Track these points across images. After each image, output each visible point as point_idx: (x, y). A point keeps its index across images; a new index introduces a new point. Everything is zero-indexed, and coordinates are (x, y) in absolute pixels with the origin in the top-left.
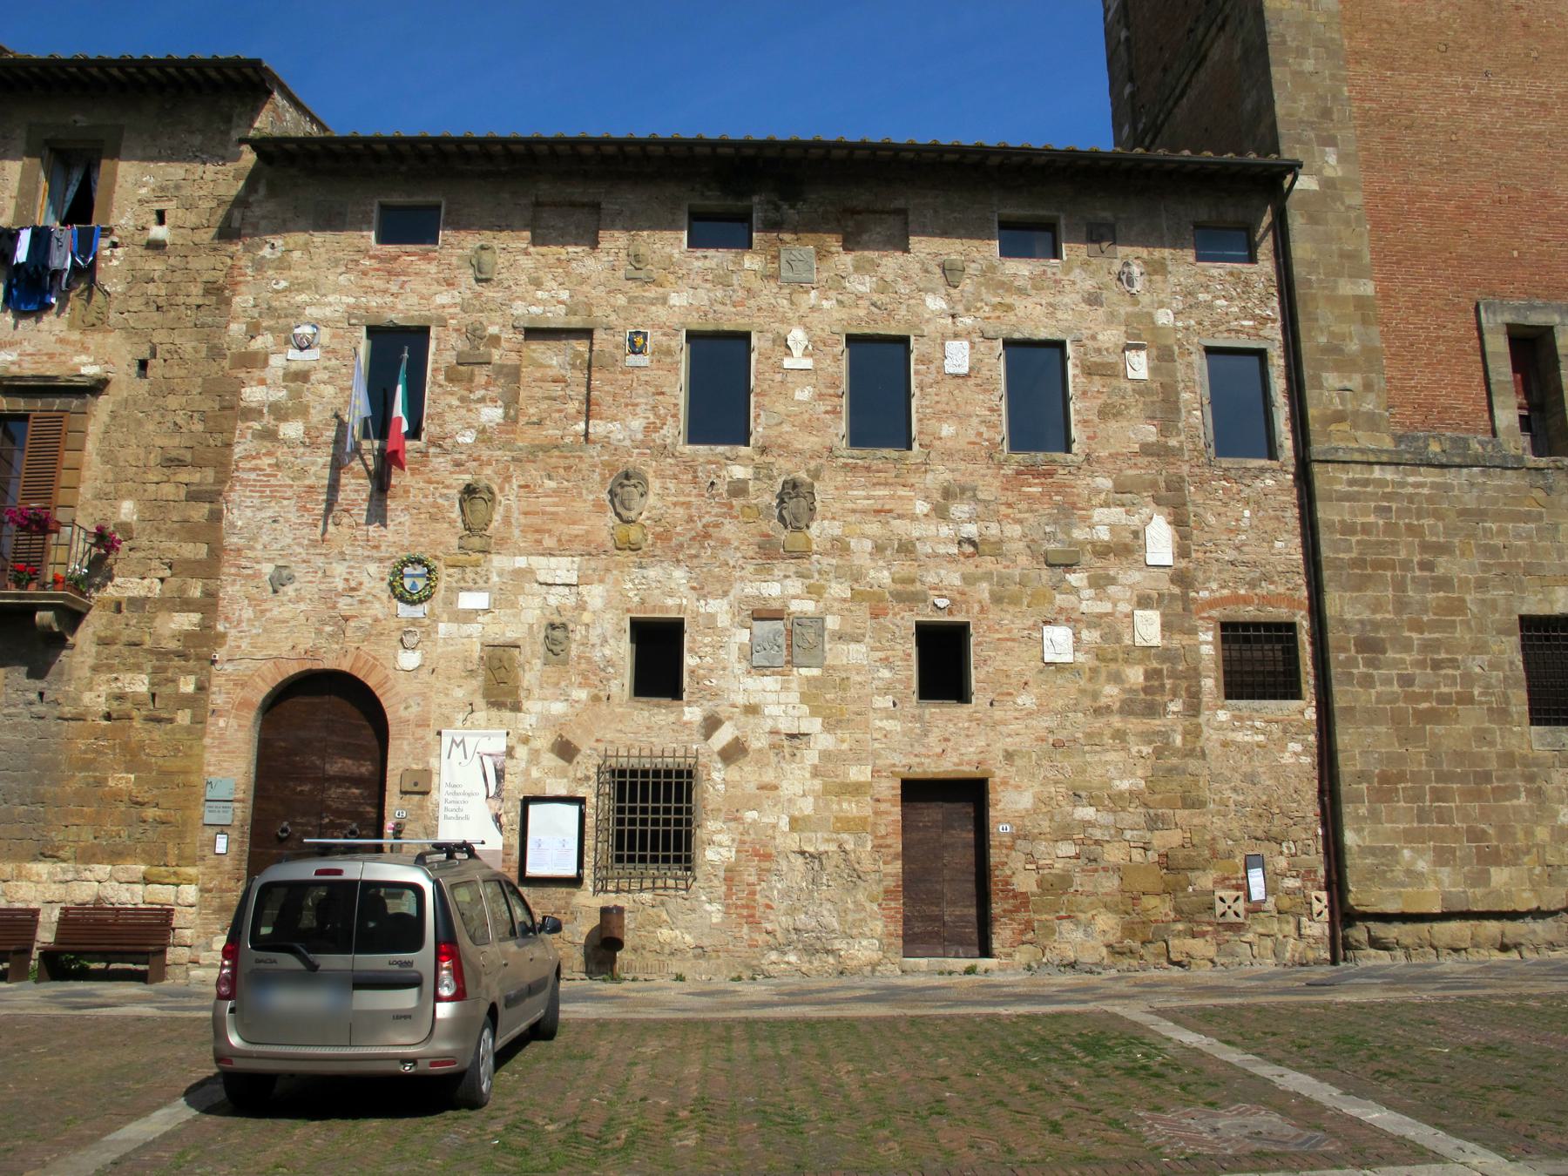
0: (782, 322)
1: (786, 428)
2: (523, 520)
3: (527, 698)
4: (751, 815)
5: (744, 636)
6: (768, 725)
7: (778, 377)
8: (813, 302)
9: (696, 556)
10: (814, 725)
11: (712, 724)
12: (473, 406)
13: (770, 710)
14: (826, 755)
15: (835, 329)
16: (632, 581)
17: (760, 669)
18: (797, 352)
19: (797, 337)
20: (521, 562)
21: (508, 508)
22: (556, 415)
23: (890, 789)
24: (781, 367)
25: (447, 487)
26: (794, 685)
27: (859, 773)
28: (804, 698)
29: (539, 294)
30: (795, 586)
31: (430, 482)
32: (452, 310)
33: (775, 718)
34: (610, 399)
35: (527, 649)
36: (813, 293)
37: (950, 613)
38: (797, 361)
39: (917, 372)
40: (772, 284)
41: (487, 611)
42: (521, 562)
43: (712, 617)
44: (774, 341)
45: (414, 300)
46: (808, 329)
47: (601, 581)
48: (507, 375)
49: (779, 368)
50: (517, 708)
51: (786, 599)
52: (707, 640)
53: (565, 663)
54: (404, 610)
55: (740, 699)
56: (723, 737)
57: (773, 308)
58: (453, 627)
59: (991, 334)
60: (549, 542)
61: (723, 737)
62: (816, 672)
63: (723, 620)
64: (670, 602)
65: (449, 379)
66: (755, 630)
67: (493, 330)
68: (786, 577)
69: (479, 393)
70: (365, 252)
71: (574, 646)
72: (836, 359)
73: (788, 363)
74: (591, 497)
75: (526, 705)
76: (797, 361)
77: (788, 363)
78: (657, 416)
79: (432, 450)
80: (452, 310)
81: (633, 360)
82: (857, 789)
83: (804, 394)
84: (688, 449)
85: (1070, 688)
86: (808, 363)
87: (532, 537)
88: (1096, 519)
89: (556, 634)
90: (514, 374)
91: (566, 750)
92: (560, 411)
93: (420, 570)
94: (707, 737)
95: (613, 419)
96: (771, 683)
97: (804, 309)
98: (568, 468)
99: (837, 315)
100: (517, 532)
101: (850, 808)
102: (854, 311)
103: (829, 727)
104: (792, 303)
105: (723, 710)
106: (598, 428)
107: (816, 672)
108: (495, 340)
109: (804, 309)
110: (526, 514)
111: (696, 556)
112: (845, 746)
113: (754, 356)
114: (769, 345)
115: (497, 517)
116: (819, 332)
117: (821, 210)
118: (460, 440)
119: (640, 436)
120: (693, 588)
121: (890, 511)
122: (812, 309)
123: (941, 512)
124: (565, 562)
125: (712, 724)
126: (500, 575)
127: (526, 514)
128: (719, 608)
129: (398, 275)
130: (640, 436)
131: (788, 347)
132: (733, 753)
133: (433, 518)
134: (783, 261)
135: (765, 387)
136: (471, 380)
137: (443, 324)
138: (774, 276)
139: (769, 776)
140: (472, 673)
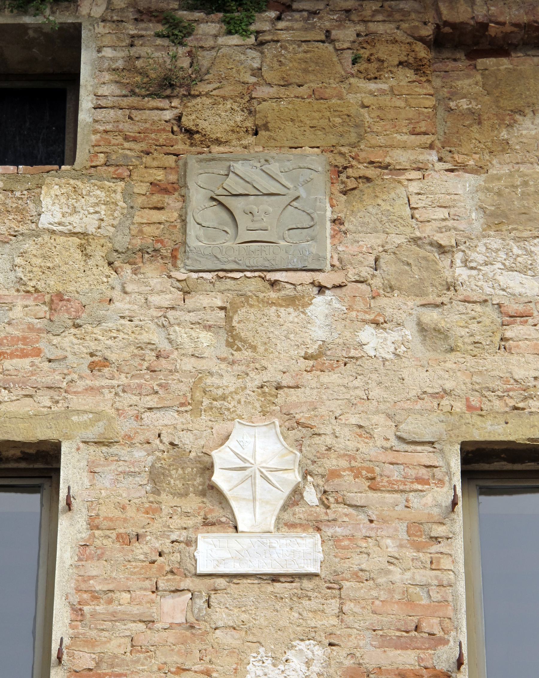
0: (189, 405)
7: (173, 609)
8: (318, 333)
15: (412, 427)
19: (254, 457)
24: (185, 570)
36: (321, 306)
38: (256, 542)
40: (153, 275)
44: (157, 477)
46: (299, 429)
49: (175, 572)
57: (155, 361)
72: (422, 535)
73: (212, 553)
76: (256, 542)
77: (212, 553)
86: (302, 552)
97: (282, 360)
99: (418, 379)
102: (495, 363)
104: (234, 340)
109: (282, 360)
113: (69, 531)
114: (135, 490)
116: (347, 441)
117: (346, 35)
122: (318, 359)
131: (213, 491)
134: (197, 196)
135: (116, 646)
138: (166, 252)
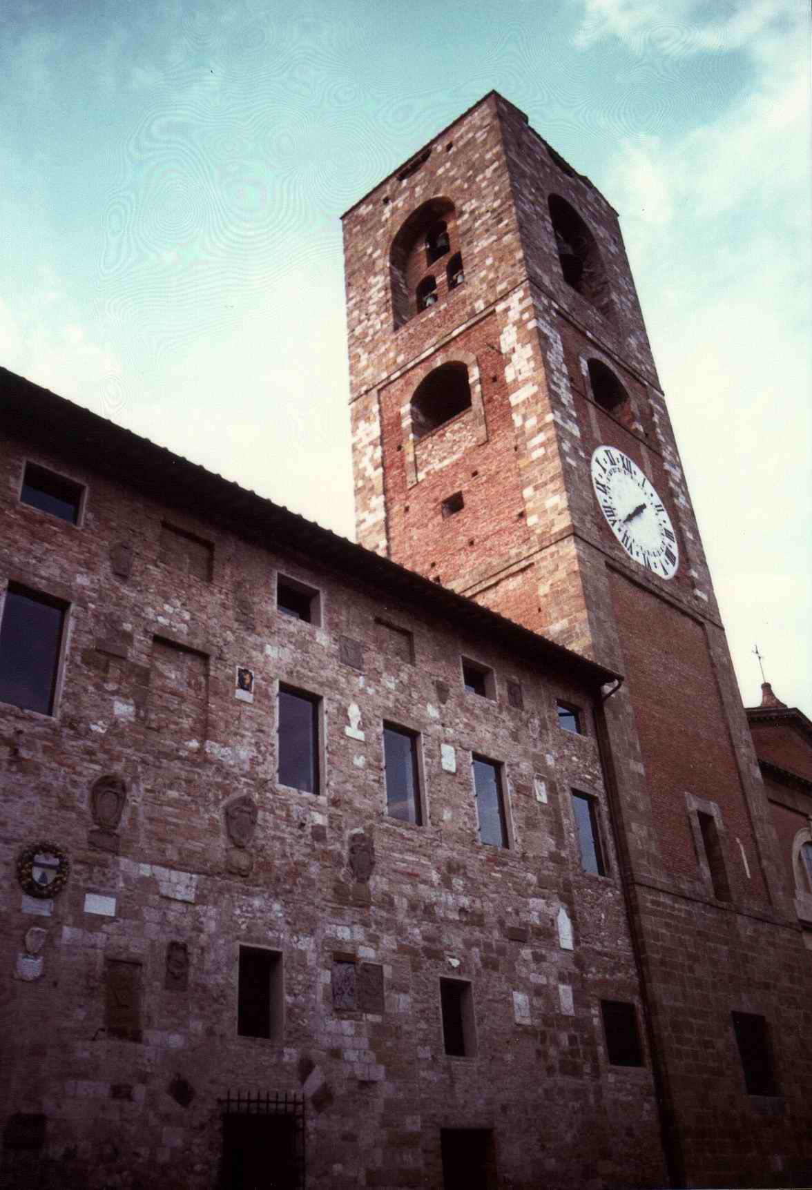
1: (349, 787)
2: (149, 827)
3: (148, 1027)
4: (338, 1167)
5: (325, 977)
6: (347, 1070)
7: (342, 742)
9: (290, 891)
10: (379, 1073)
11: (306, 1067)
12: (106, 696)
13: (350, 1055)
14: (389, 1104)
16: (240, 907)
17: (339, 1013)
18: (354, 724)
19: (354, 711)
20: (146, 870)
21: (134, 809)
22: (173, 726)
23: (432, 1139)
25: (80, 774)
26: (364, 1030)
27: (413, 1124)
28: (374, 1045)
29: (167, 607)
30: (359, 934)
31: (61, 764)
32: (92, 594)
33: (352, 1063)
34: (222, 725)
35: (148, 970)
37: (459, 973)
38: (353, 731)
39: (427, 763)
41: (112, 920)
42: (146, 870)
43: (302, 954)
45: (57, 572)
47: (215, 904)
48: (138, 675)
50: (137, 1037)
51: (354, 943)
52: (300, 977)
53: (184, 989)
54: (30, 906)
55: (326, 1041)
56: (315, 1080)
58: (78, 932)
59: (465, 746)
60: (172, 854)
61: (315, 1080)
62: (377, 1019)
63: (311, 958)
64: (270, 934)
65: (84, 661)
66: (336, 970)
67: (128, 627)
68: (354, 923)
69: (111, 687)
70: (12, 504)
71: (191, 970)
74: (206, 816)
75: (147, 1034)
78: (260, 752)
79: (66, 731)
80: (92, 594)
81: (241, 694)
82: (409, 1141)
83: (360, 761)
84: (282, 788)
85: (531, 1047)
86: (360, 735)
87: (155, 844)
88: (531, 906)
89: (178, 954)
90: (145, 675)
91: (182, 1091)
92: (177, 724)
93: (56, 862)
94: (303, 1080)
95: (225, 744)
96: (347, 1026)
98: (189, 782)
100: (142, 836)
101: (411, 1160)
103: (390, 1075)
105: (317, 1054)
106: (214, 749)
107: (377, 1019)
108: (128, 637)
110: (151, 820)
111: (290, 891)
112: (401, 1095)
115: (125, 818)
118: (94, 727)
119: (247, 767)
120: (288, 923)
121: (417, 875)
123: (446, 883)
124: (184, 876)
125: (306, 1067)
126: (127, 880)
127: (151, 820)
128: (306, 944)
129: (43, 540)
130: (247, 767)
132: (324, 1099)
133: (63, 806)
136: (106, 670)
137: (83, 603)
139: (349, 1126)
140: (91, 991)
